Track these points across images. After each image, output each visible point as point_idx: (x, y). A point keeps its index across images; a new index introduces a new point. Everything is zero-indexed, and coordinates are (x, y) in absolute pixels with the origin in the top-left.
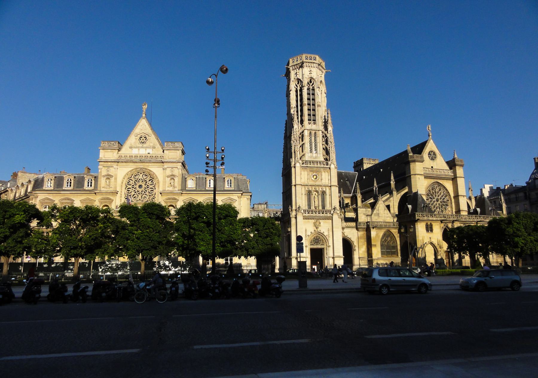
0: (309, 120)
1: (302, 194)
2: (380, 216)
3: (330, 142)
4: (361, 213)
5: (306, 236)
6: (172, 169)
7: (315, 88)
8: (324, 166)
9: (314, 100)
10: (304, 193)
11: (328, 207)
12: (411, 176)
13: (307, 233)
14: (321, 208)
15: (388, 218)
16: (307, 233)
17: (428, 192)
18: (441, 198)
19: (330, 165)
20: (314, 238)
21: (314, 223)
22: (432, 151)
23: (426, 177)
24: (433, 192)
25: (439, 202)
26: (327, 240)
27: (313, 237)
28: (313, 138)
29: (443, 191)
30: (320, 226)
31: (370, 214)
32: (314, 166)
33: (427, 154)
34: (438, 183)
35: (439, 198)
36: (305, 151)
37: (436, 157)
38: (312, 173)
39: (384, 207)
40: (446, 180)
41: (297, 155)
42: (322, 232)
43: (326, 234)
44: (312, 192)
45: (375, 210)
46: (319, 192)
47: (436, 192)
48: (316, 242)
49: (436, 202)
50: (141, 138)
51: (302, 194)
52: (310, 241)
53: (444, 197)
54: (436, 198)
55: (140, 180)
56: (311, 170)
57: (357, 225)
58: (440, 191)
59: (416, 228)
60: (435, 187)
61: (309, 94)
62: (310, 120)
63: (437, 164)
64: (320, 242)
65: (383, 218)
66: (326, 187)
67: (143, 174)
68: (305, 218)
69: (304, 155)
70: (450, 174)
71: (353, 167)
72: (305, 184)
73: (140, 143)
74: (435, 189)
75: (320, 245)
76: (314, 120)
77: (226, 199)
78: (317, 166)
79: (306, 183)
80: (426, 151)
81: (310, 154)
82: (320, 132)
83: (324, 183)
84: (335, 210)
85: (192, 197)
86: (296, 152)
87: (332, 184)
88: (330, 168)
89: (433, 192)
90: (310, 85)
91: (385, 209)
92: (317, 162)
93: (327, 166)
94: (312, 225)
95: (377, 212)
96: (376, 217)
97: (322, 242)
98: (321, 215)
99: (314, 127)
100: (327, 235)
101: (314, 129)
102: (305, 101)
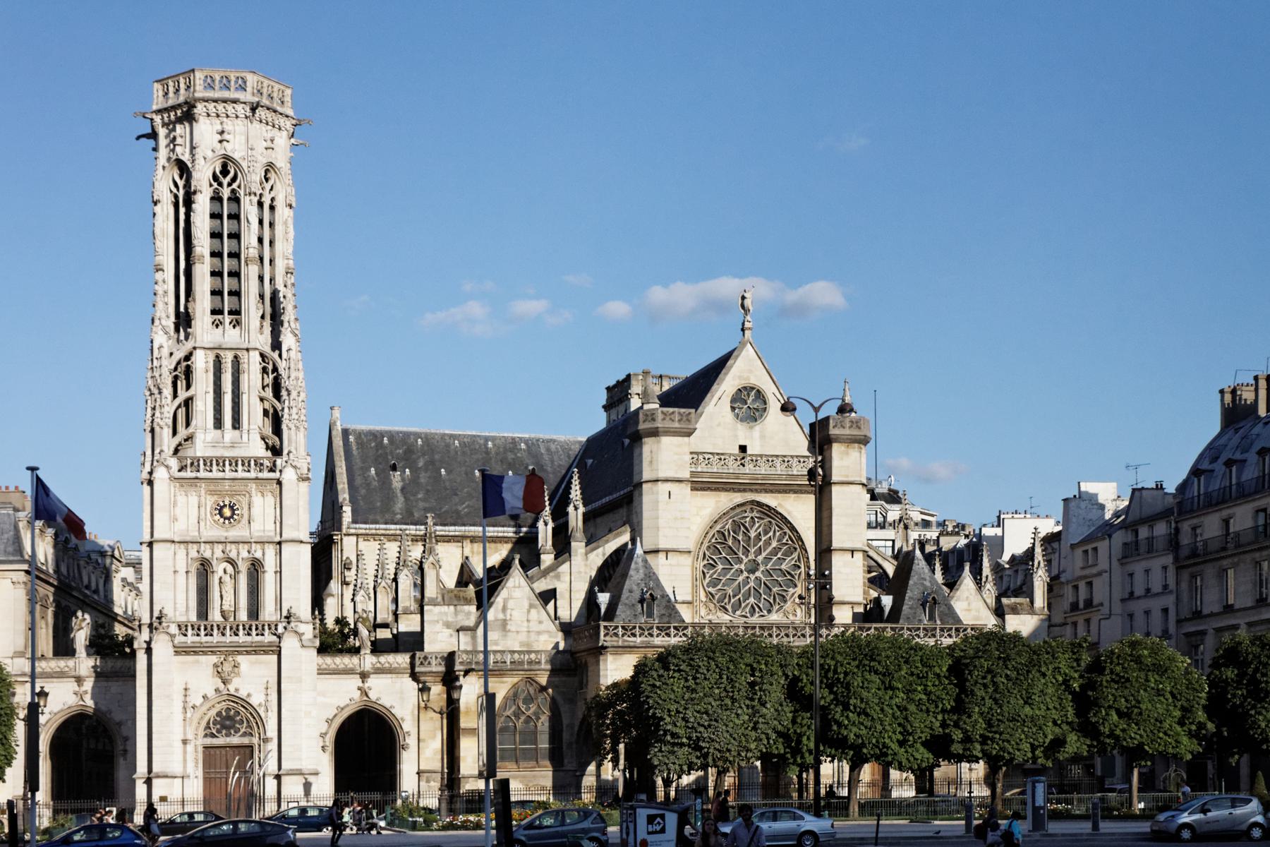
1: (175, 572)
2: (509, 631)
3: (287, 390)
4: (438, 622)
5: (185, 708)
8: (260, 475)
10: (182, 566)
11: (269, 612)
12: (644, 486)
13: (188, 699)
14: (243, 616)
17: (713, 541)
18: (767, 559)
19: (281, 471)
20: (219, 714)
21: (215, 666)
23: (699, 485)
25: (758, 574)
26: (261, 723)
27: (213, 712)
29: (778, 534)
30: (238, 674)
31: (471, 622)
32: (221, 475)
34: (759, 504)
35: (760, 559)
38: (215, 496)
39: (529, 599)
40: (795, 492)
41: (161, 440)
42: (243, 694)
43: (255, 701)
44: (214, 563)
46: (240, 563)
47: (749, 537)
48: (224, 727)
49: (745, 574)
51: (175, 572)
52: (204, 724)
53: (779, 556)
54: (745, 560)
56: (212, 488)
57: (412, 665)
58: (766, 533)
59: (602, 673)
60: (748, 519)
62: (220, 312)
64: (238, 726)
65: (523, 637)
66: (266, 545)
68: (180, 651)
69: (189, 438)
72: (188, 539)
78: (234, 475)
79: (193, 534)
81: (214, 434)
82: (255, 357)
83: (258, 531)
84: (289, 623)
86: (157, 429)
87: (285, 536)
88: (279, 483)
91: (531, 606)
92: (234, 462)
93: (272, 475)
94: (210, 670)
95: (501, 616)
97: (245, 724)
98: (242, 638)
100: (260, 705)
101: (228, 347)
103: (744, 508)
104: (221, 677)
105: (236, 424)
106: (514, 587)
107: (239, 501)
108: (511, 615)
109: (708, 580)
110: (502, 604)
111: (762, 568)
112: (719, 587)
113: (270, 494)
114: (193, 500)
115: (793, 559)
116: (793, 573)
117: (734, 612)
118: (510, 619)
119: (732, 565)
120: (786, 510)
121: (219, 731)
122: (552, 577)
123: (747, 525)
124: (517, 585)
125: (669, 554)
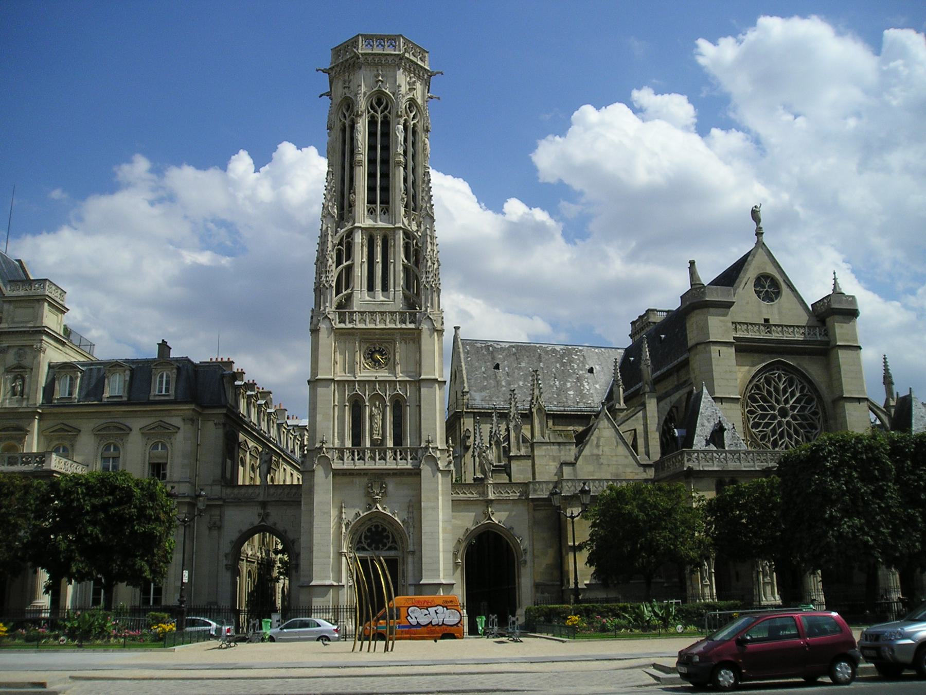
2: (602, 464)
6: (20, 349)
7: (392, 117)
9: (386, 148)
14: (390, 443)
15: (629, 470)
17: (753, 392)
20: (369, 530)
22: (770, 277)
24: (769, 392)
27: (364, 529)
28: (379, 250)
29: (799, 387)
33: (751, 285)
35: (788, 406)
36: (351, 286)
37: (778, 294)
39: (615, 438)
44: (366, 399)
45: (587, 447)
46: (387, 399)
49: (779, 418)
52: (357, 537)
53: (802, 404)
60: (777, 375)
61: (372, 134)
63: (780, 313)
70: (819, 339)
71: (630, 335)
74: (775, 382)
75: (385, 548)
76: (385, 201)
77: (152, 426)
80: (748, 276)
85: (65, 422)
89: (769, 392)
90: (376, 112)
95: (595, 451)
96: (591, 468)
102: (363, 155)
103: (772, 367)
104: (371, 497)
105: (385, 288)
106: (604, 428)
107: (387, 347)
108: (603, 451)
109: (751, 422)
110: (595, 442)
111: (791, 413)
112: (760, 429)
113: (411, 342)
115: (812, 407)
116: (813, 417)
117: (774, 448)
118: (602, 455)
119: (768, 411)
120: (806, 371)
121: (369, 545)
122: (633, 420)
123: (776, 379)
124: (607, 426)
125: (723, 400)
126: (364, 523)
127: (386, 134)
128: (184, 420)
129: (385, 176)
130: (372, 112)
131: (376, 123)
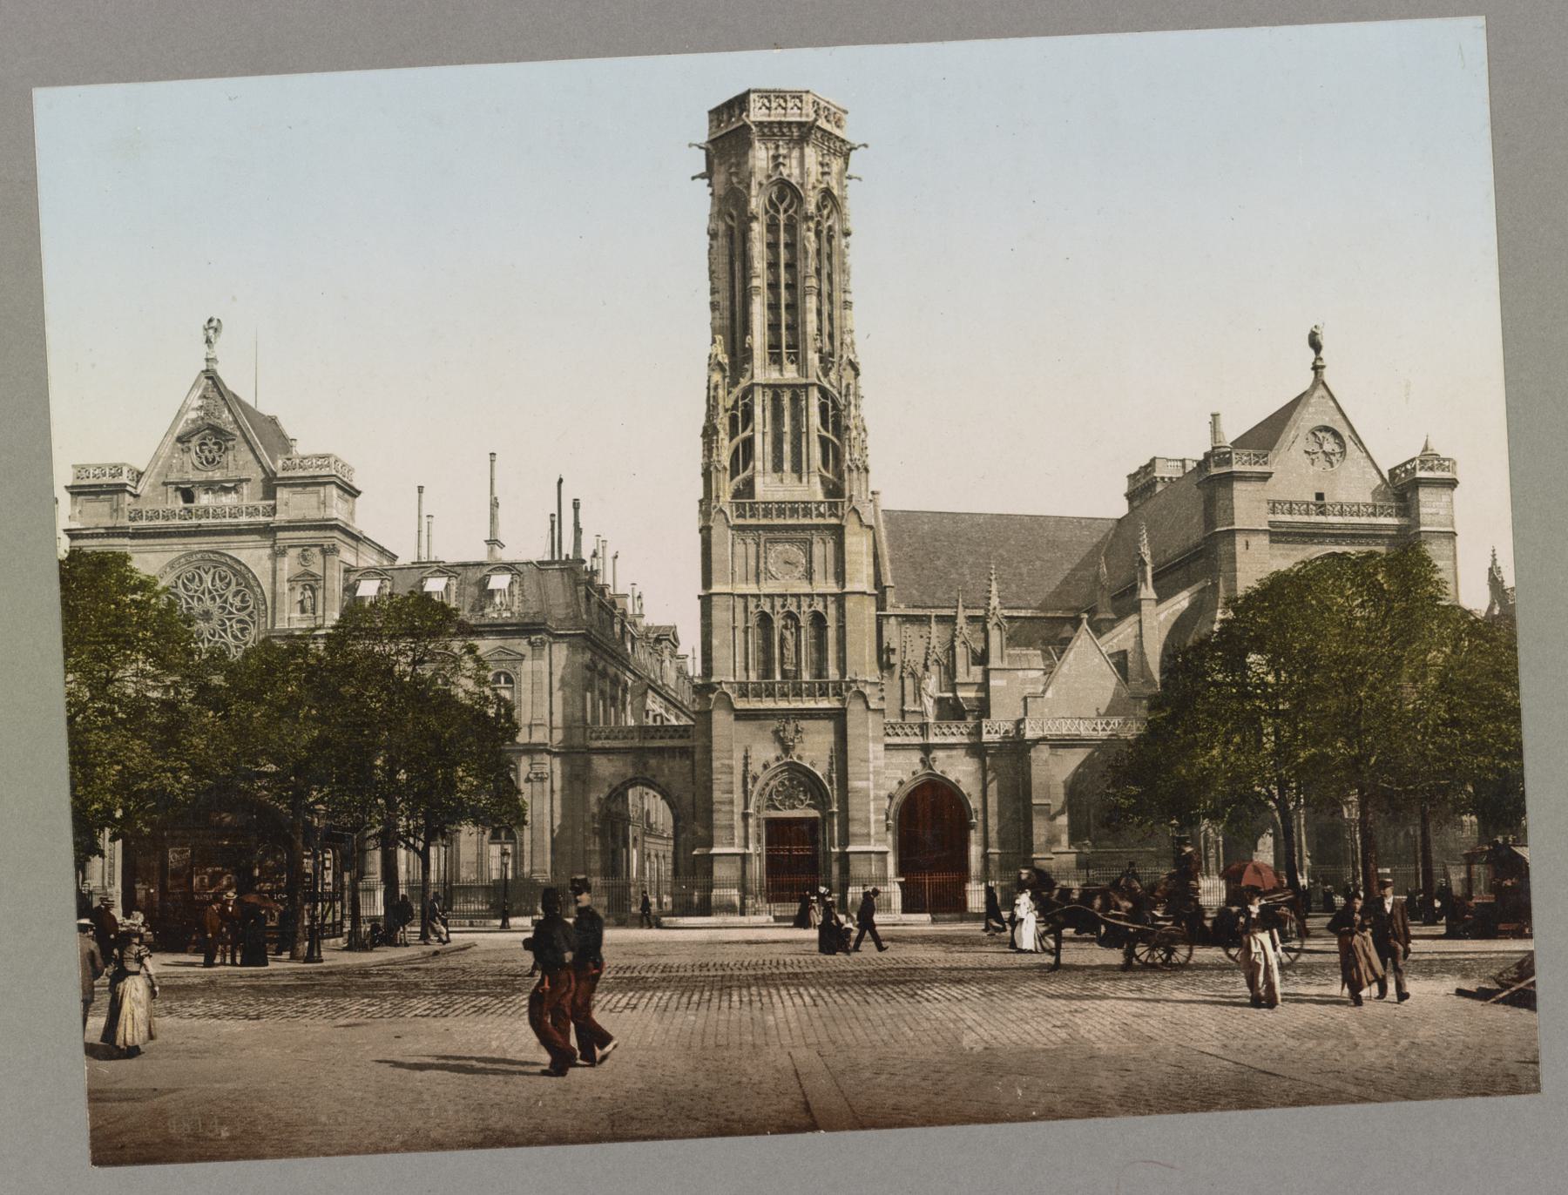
0: (771, 347)
1: (734, 628)
6: (304, 550)
11: (833, 673)
16: (749, 768)
20: (782, 784)
21: (776, 732)
50: (204, 447)
55: (203, 593)
61: (773, 246)
67: (212, 570)
68: (743, 716)
73: (202, 463)
76: (793, 346)
81: (771, 478)
90: (778, 211)
99: (790, 374)
105: (797, 468)
114: (752, 549)
126: (776, 775)
127: (791, 246)
128: (530, 643)
129: (792, 307)
130: (772, 212)
131: (778, 225)
